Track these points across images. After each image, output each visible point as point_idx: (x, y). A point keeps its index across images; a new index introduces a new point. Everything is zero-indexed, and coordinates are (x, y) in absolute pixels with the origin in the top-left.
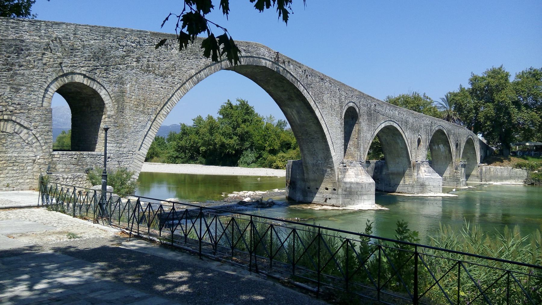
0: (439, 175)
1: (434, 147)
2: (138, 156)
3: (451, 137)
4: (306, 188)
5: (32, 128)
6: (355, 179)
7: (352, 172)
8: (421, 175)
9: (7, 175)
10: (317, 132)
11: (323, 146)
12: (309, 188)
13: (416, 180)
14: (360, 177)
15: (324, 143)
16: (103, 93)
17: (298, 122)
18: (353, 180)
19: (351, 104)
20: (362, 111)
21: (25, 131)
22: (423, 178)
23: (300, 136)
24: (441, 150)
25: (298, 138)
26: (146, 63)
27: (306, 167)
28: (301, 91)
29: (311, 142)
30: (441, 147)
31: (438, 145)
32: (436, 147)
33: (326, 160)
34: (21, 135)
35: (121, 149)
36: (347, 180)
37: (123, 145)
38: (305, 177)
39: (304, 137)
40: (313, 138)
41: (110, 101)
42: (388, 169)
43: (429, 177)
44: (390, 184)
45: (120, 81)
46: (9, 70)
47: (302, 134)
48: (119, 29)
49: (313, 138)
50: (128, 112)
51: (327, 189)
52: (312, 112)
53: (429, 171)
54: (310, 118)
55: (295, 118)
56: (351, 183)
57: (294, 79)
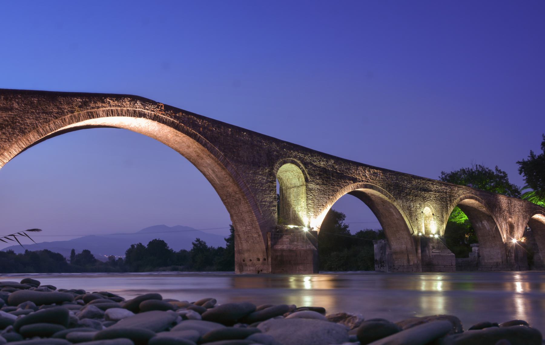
0: (451, 252)
1: (477, 225)
4: (242, 261)
6: (288, 245)
7: (287, 238)
8: (427, 252)
10: (237, 192)
11: (246, 208)
12: (244, 261)
13: (420, 258)
14: (296, 243)
15: (246, 205)
17: (218, 182)
18: (285, 247)
22: (430, 256)
23: (226, 199)
24: (485, 228)
25: (225, 202)
27: (239, 235)
30: (485, 224)
31: (482, 222)
32: (480, 225)
33: (253, 224)
36: (279, 247)
38: (240, 248)
42: (390, 248)
44: (394, 266)
47: (226, 197)
51: (258, 260)
53: (438, 247)
54: (225, 176)
56: (282, 250)
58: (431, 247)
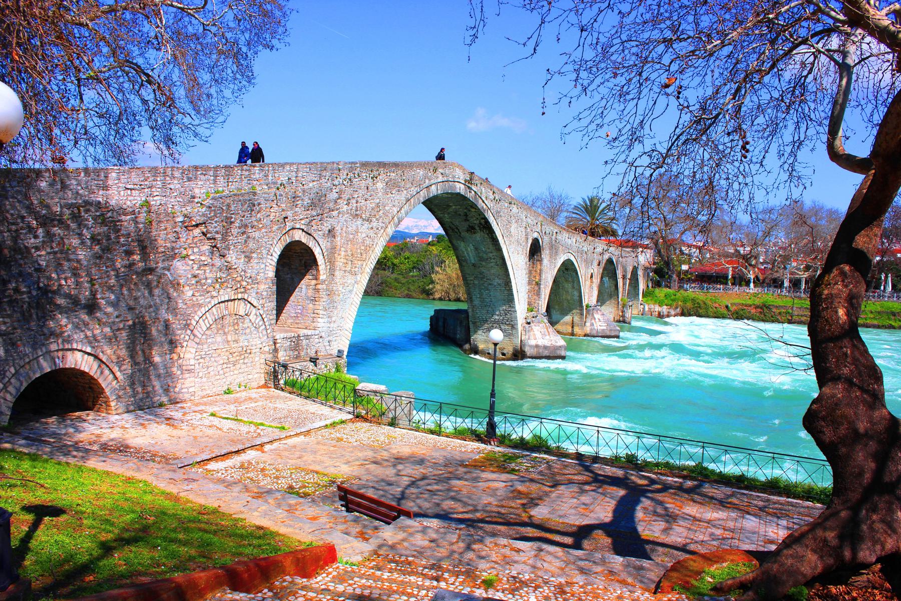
2: (346, 332)
3: (619, 266)
5: (260, 307)
9: (240, 371)
16: (317, 252)
19: (536, 235)
20: (545, 242)
21: (254, 311)
26: (355, 205)
28: (491, 222)
29: (487, 290)
34: (251, 317)
35: (332, 325)
37: (333, 319)
39: (476, 282)
40: (490, 284)
41: (323, 261)
43: (605, 328)
45: (331, 232)
46: (243, 233)
48: (333, 163)
49: (490, 284)
50: (338, 273)
52: (499, 249)
55: (469, 255)
57: (485, 207)
58: (597, 320)
